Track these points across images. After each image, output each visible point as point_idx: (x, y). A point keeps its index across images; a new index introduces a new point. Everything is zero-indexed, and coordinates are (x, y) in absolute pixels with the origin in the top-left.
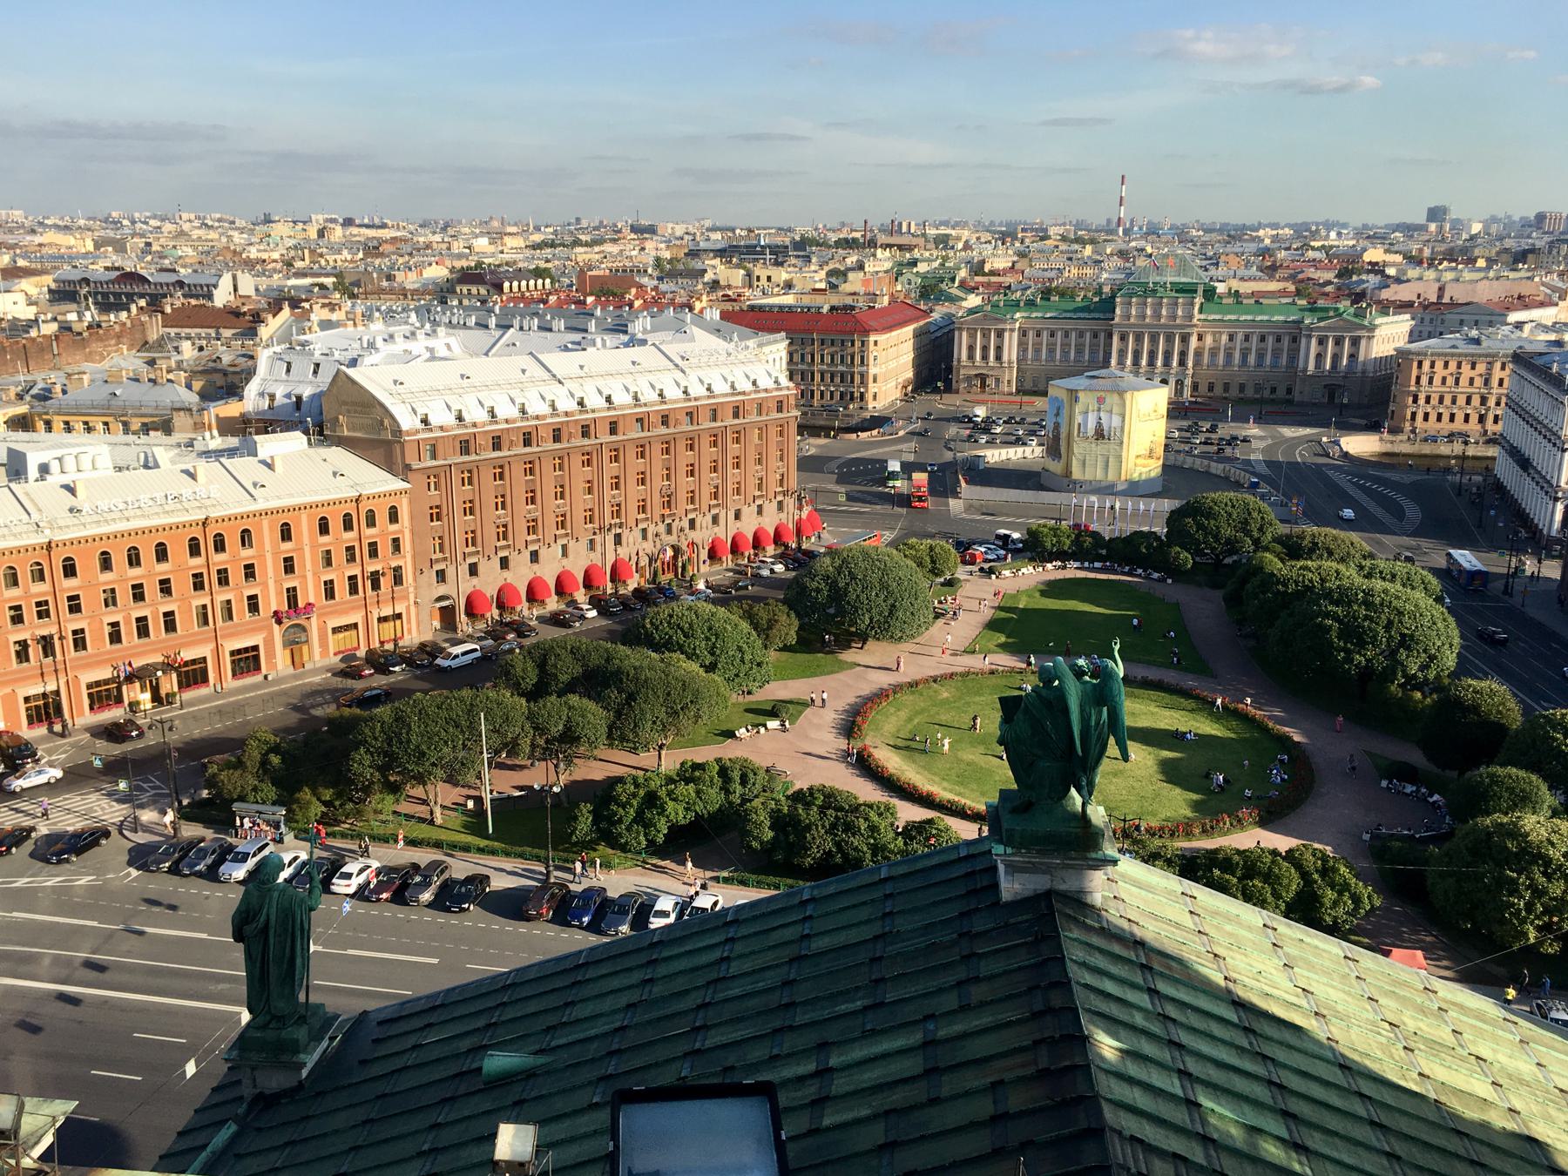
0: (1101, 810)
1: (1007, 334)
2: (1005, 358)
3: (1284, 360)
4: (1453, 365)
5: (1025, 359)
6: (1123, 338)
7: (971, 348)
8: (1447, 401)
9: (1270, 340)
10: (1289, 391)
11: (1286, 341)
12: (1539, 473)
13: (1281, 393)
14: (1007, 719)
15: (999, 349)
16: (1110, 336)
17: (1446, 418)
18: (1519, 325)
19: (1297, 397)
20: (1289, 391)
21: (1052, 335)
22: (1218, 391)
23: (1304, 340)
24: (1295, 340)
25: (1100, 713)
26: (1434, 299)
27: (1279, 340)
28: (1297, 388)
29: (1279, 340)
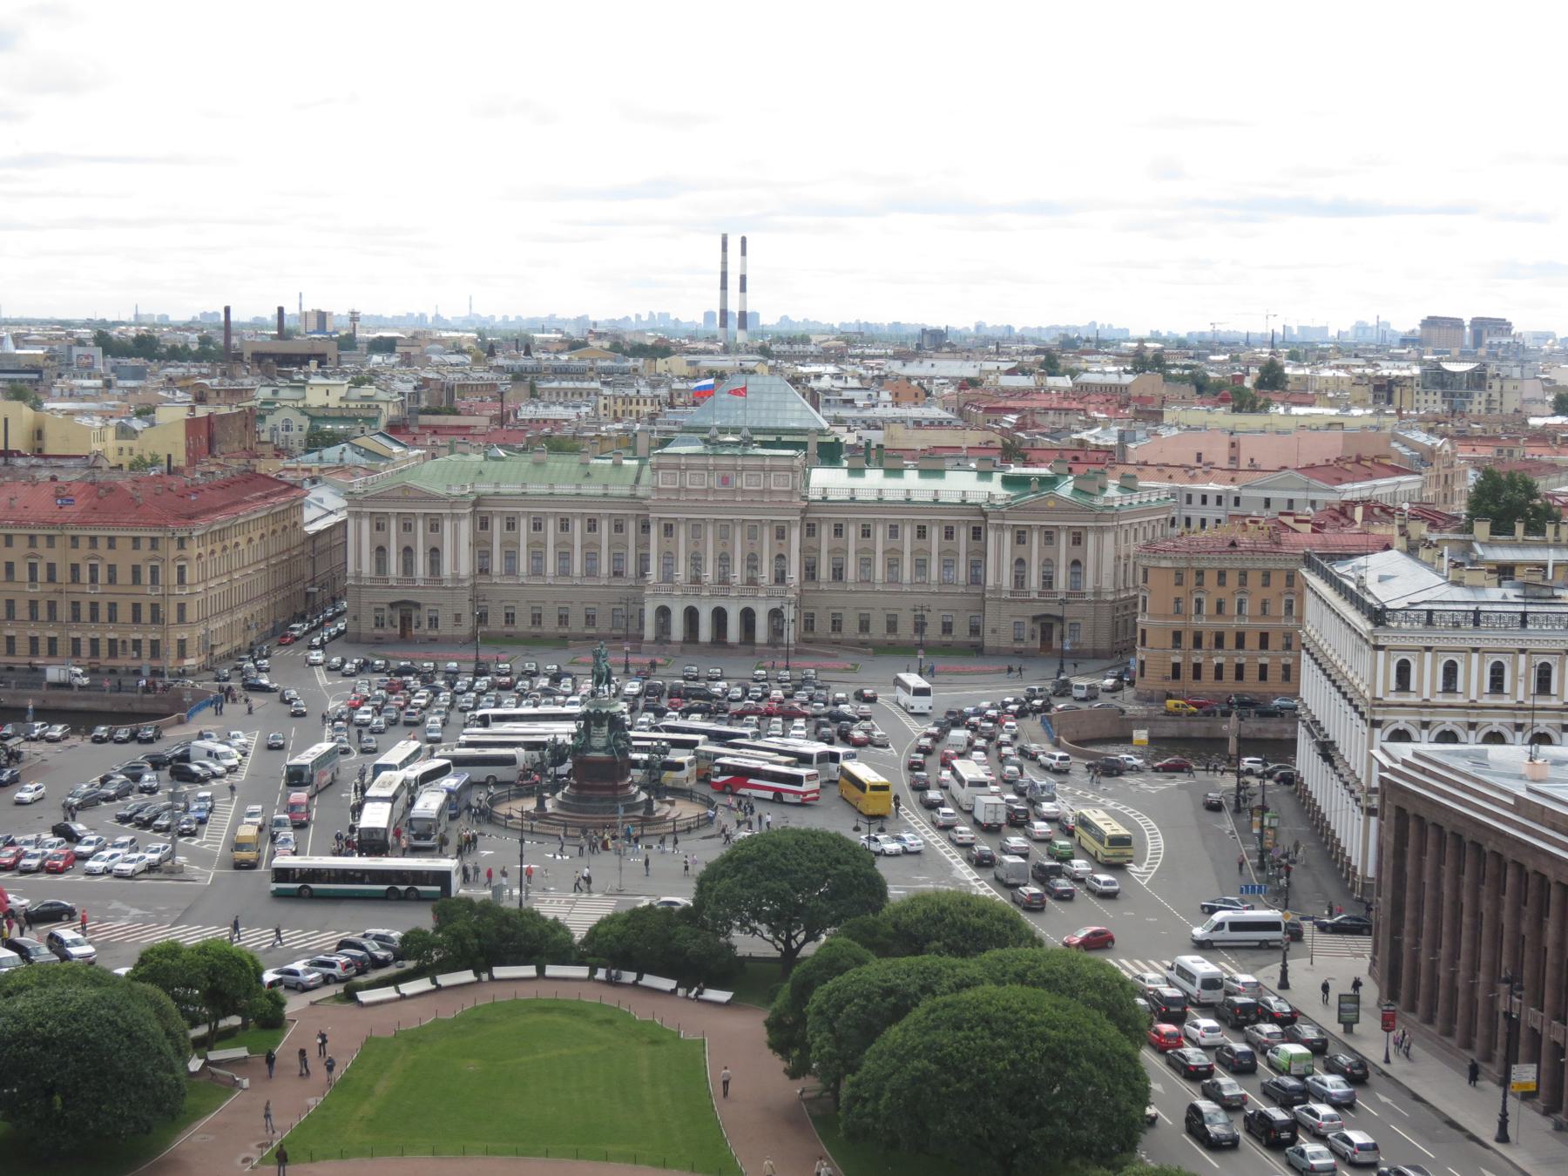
1: (447, 526)
2: (447, 570)
3: (961, 572)
4: (1232, 580)
5: (484, 571)
6: (669, 529)
7: (381, 551)
8: (1230, 641)
9: (935, 535)
10: (975, 630)
11: (963, 535)
12: (1347, 765)
13: (961, 633)
15: (435, 553)
16: (646, 528)
17: (1229, 673)
18: (1343, 512)
19: (989, 641)
20: (975, 630)
21: (537, 527)
22: (850, 629)
23: (991, 535)
24: (977, 533)
26: (1223, 462)
27: (949, 533)
28: (989, 622)
29: (949, 533)
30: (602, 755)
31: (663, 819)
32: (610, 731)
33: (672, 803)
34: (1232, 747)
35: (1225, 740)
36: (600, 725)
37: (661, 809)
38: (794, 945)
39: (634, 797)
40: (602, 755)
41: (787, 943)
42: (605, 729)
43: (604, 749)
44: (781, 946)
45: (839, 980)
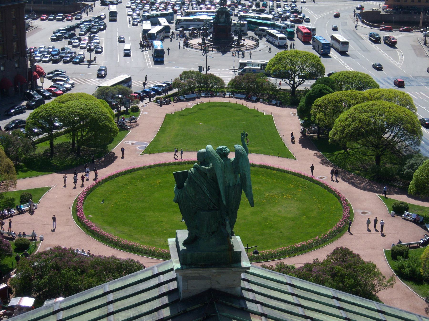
0: (238, 237)
14: (180, 187)
25: (236, 177)
30: (223, 25)
31: (242, 46)
32: (226, 17)
33: (244, 40)
34: (421, 24)
35: (419, 23)
36: (222, 15)
37: (242, 43)
38: (295, 86)
39: (233, 38)
40: (223, 25)
41: (293, 85)
42: (224, 16)
43: (224, 23)
44: (291, 86)
45: (323, 98)
